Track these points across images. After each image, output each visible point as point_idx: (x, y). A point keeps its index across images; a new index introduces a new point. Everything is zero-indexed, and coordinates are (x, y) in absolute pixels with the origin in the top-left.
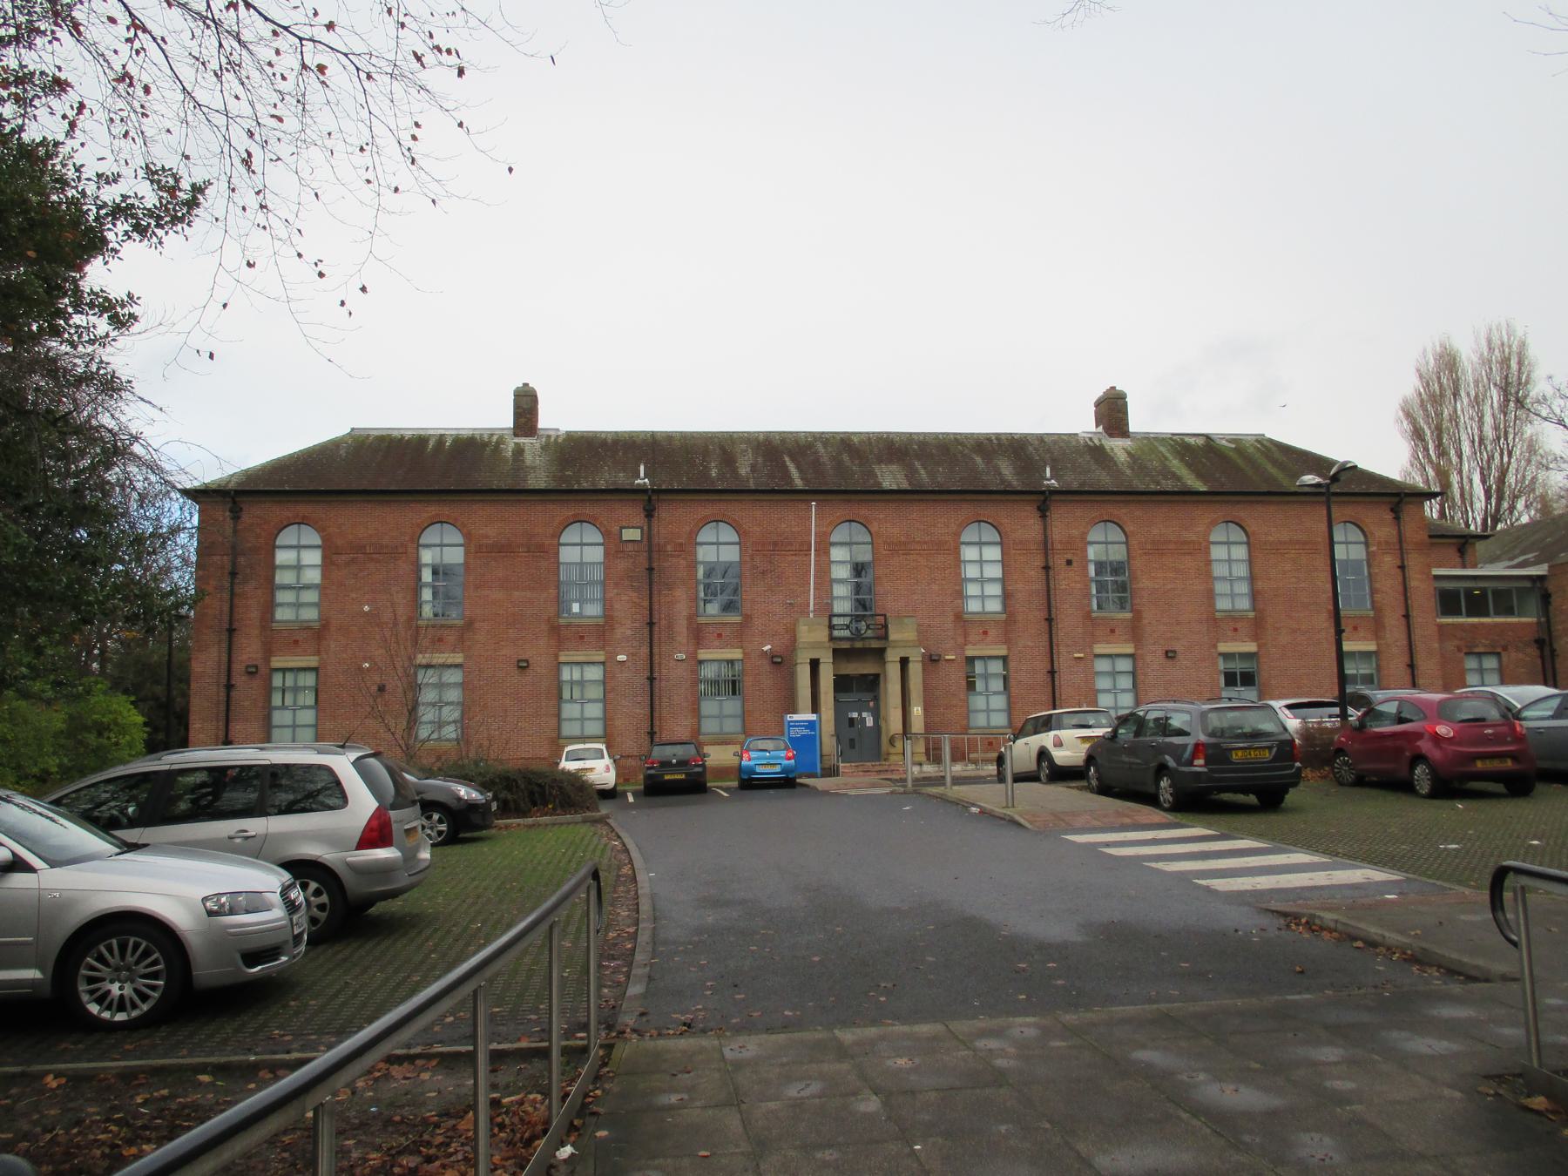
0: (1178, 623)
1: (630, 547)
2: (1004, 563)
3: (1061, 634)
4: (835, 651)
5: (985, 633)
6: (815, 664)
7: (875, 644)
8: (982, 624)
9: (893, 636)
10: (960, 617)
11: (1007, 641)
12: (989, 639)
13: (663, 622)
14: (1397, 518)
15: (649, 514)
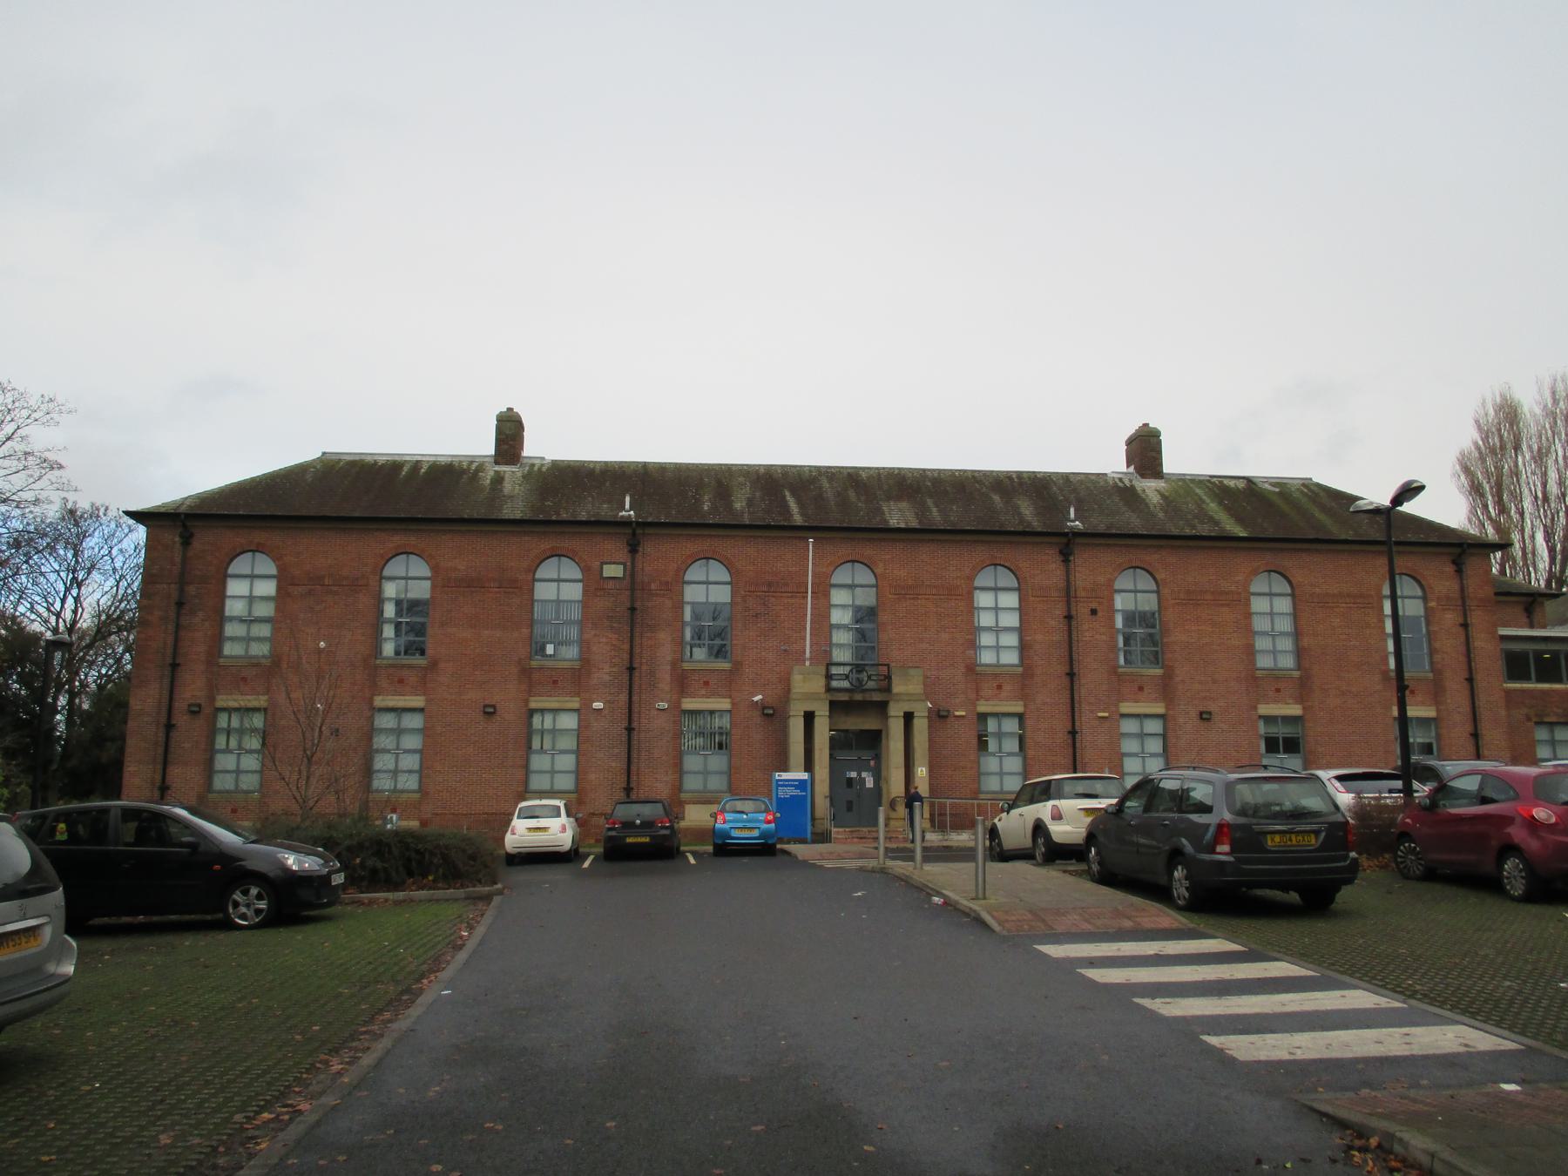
0: (1214, 681)
1: (611, 584)
2: (1022, 610)
3: (1083, 691)
4: (833, 704)
5: (999, 687)
6: (809, 717)
7: (877, 697)
8: (997, 676)
9: (898, 687)
10: (972, 669)
11: (1024, 696)
12: (1004, 694)
13: (644, 668)
14: (1459, 571)
15: (633, 549)
